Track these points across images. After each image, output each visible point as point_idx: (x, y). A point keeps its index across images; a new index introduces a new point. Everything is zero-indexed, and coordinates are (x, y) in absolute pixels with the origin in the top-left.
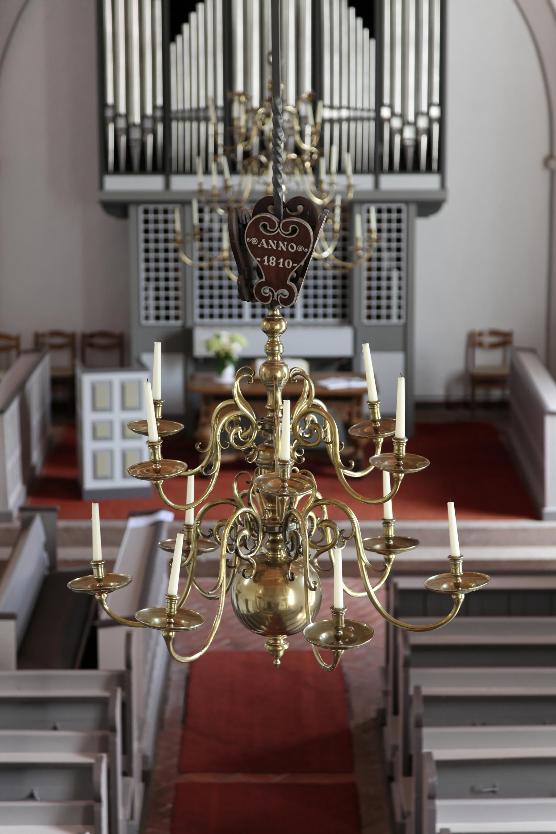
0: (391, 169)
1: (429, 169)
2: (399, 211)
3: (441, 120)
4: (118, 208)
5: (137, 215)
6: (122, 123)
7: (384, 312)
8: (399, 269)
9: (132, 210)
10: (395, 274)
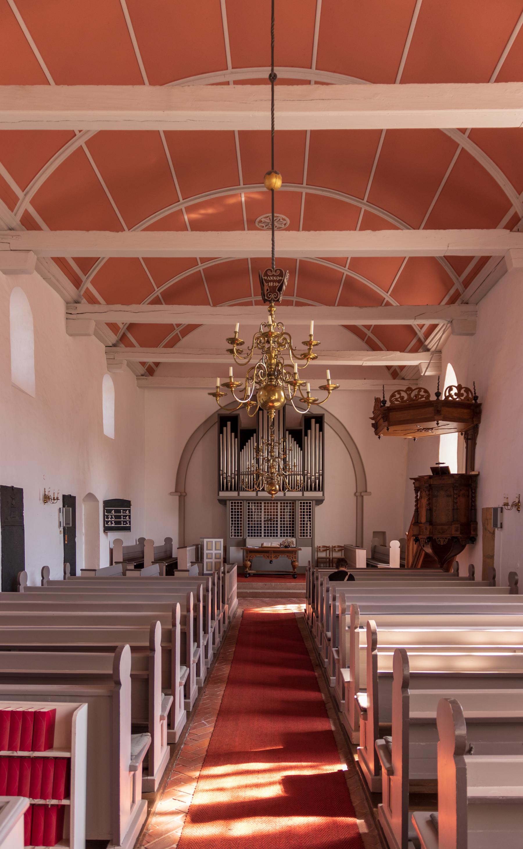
0: (307, 490)
1: (319, 490)
2: (310, 503)
3: (323, 475)
4: (223, 502)
5: (229, 504)
6: (225, 476)
7: (305, 534)
8: (310, 521)
9: (228, 502)
10: (309, 522)
